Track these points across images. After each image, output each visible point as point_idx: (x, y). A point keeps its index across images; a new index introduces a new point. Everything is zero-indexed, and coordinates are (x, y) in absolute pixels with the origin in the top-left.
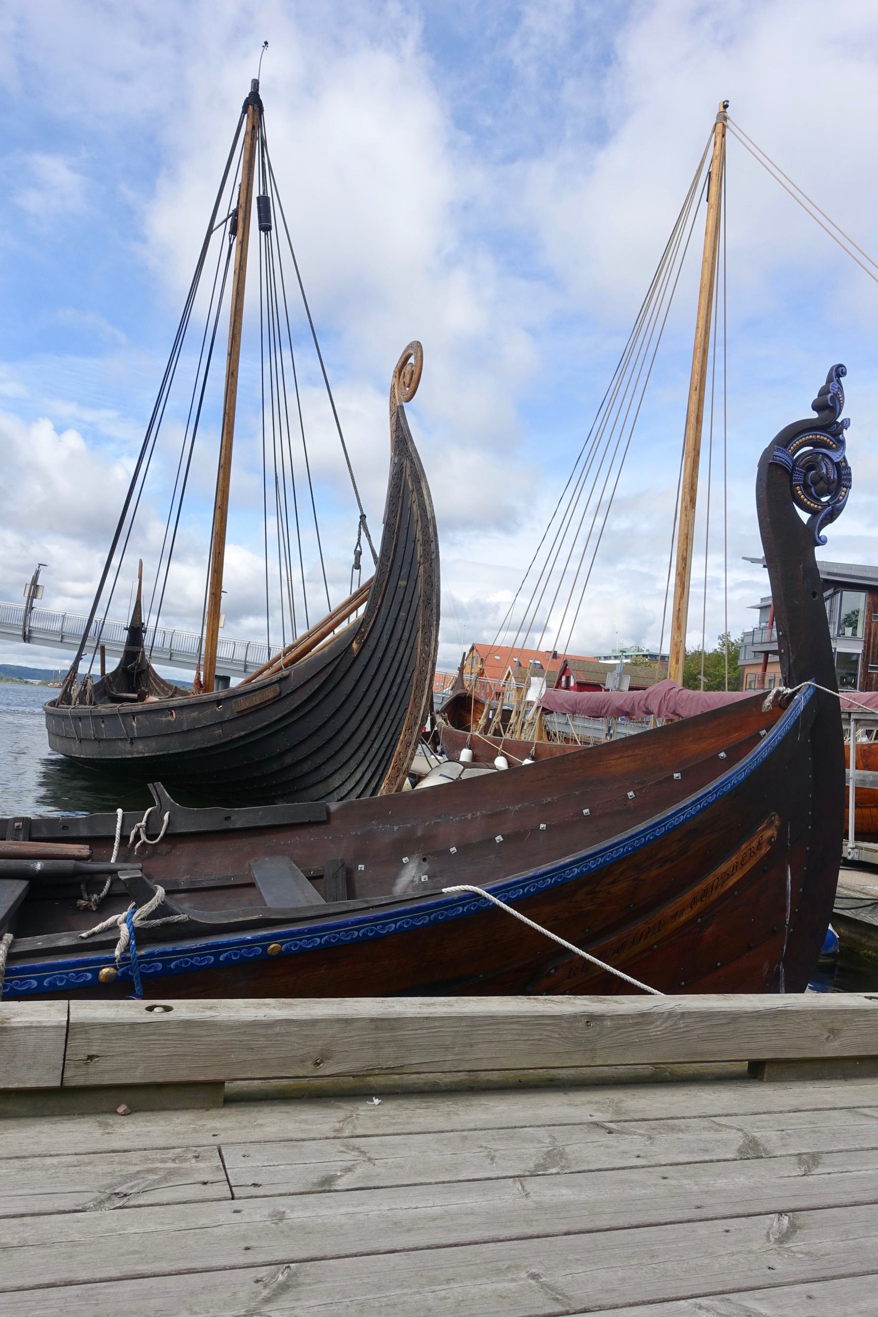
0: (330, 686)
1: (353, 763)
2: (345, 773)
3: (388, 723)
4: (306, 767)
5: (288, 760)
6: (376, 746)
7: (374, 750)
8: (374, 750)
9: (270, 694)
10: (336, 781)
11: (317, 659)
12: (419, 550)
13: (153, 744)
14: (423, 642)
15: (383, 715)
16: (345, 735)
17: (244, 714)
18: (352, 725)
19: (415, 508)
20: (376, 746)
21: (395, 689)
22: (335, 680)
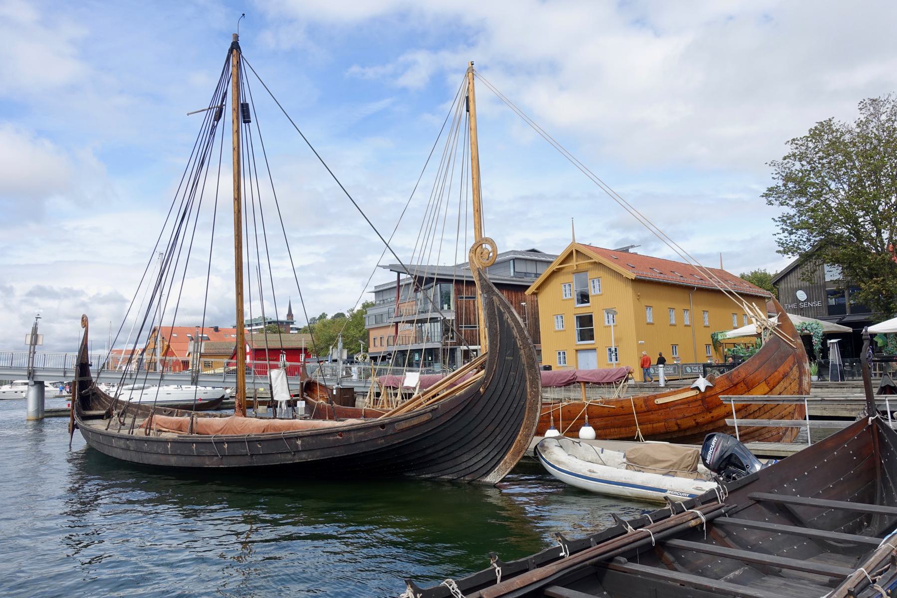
0: (466, 410)
1: (479, 448)
2: (472, 454)
3: (508, 427)
4: (442, 453)
5: (429, 451)
6: (499, 438)
7: (497, 440)
8: (497, 440)
9: (425, 418)
10: (465, 458)
11: (458, 398)
12: (519, 343)
13: (318, 453)
14: (531, 386)
15: (504, 422)
16: (474, 434)
17: (402, 431)
18: (479, 430)
19: (509, 320)
20: (499, 438)
21: (512, 410)
22: (469, 408)
